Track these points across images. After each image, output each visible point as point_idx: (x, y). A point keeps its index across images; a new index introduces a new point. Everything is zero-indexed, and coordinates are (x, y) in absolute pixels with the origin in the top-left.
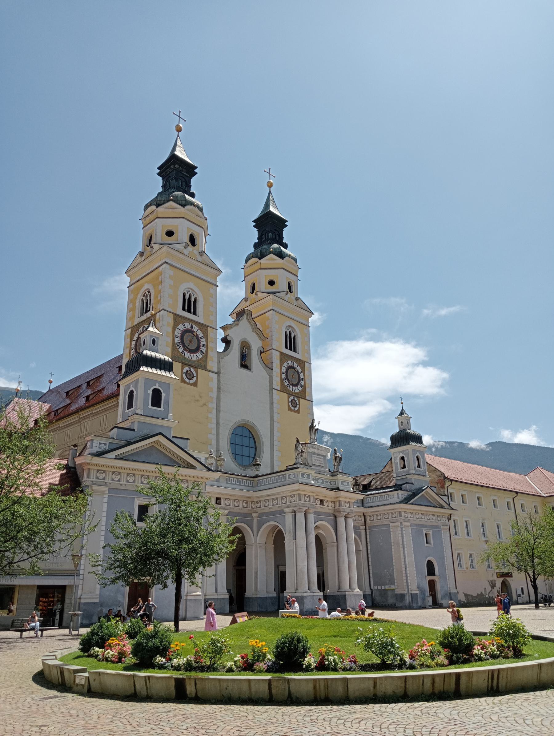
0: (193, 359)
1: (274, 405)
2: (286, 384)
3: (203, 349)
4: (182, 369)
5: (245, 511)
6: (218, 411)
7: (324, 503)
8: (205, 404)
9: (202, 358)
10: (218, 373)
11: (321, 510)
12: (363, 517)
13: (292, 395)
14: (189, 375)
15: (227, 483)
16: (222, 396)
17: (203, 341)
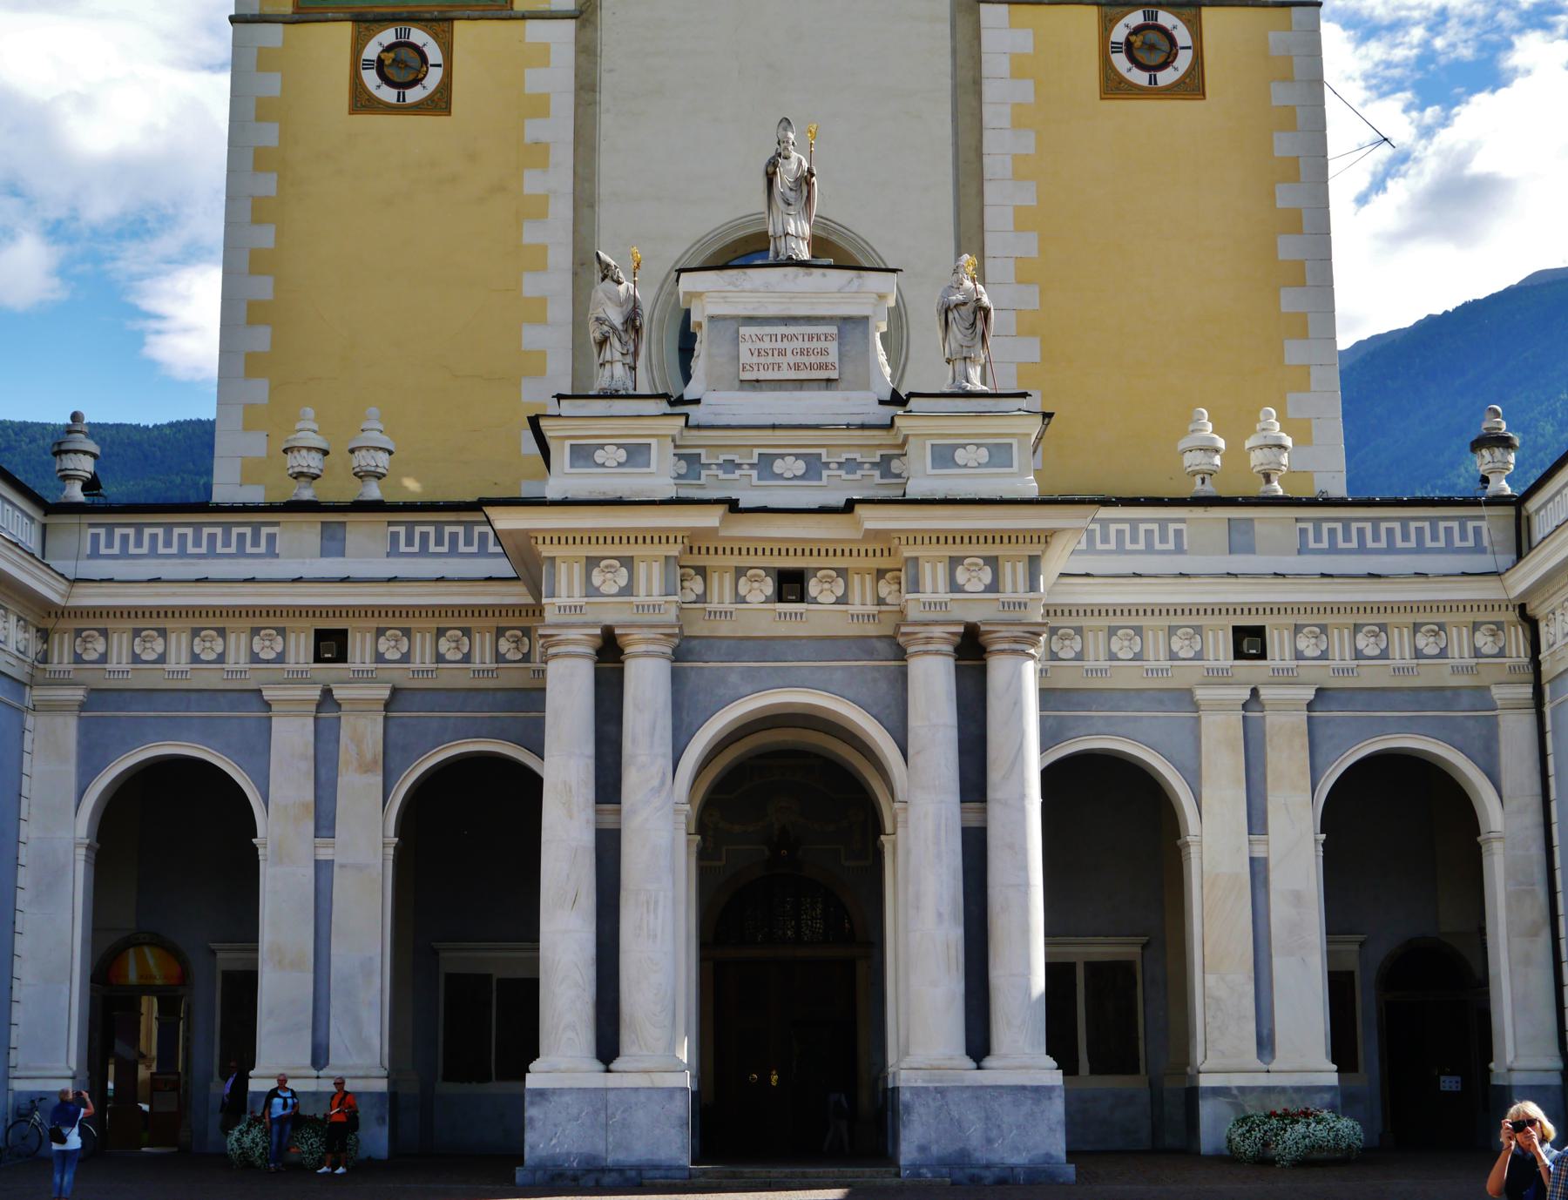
1: (990, 91)
4: (358, 46)
5: (512, 678)
6: (584, 201)
7: (813, 588)
11: (783, 629)
12: (1517, 641)
15: (393, 552)
16: (607, 123)
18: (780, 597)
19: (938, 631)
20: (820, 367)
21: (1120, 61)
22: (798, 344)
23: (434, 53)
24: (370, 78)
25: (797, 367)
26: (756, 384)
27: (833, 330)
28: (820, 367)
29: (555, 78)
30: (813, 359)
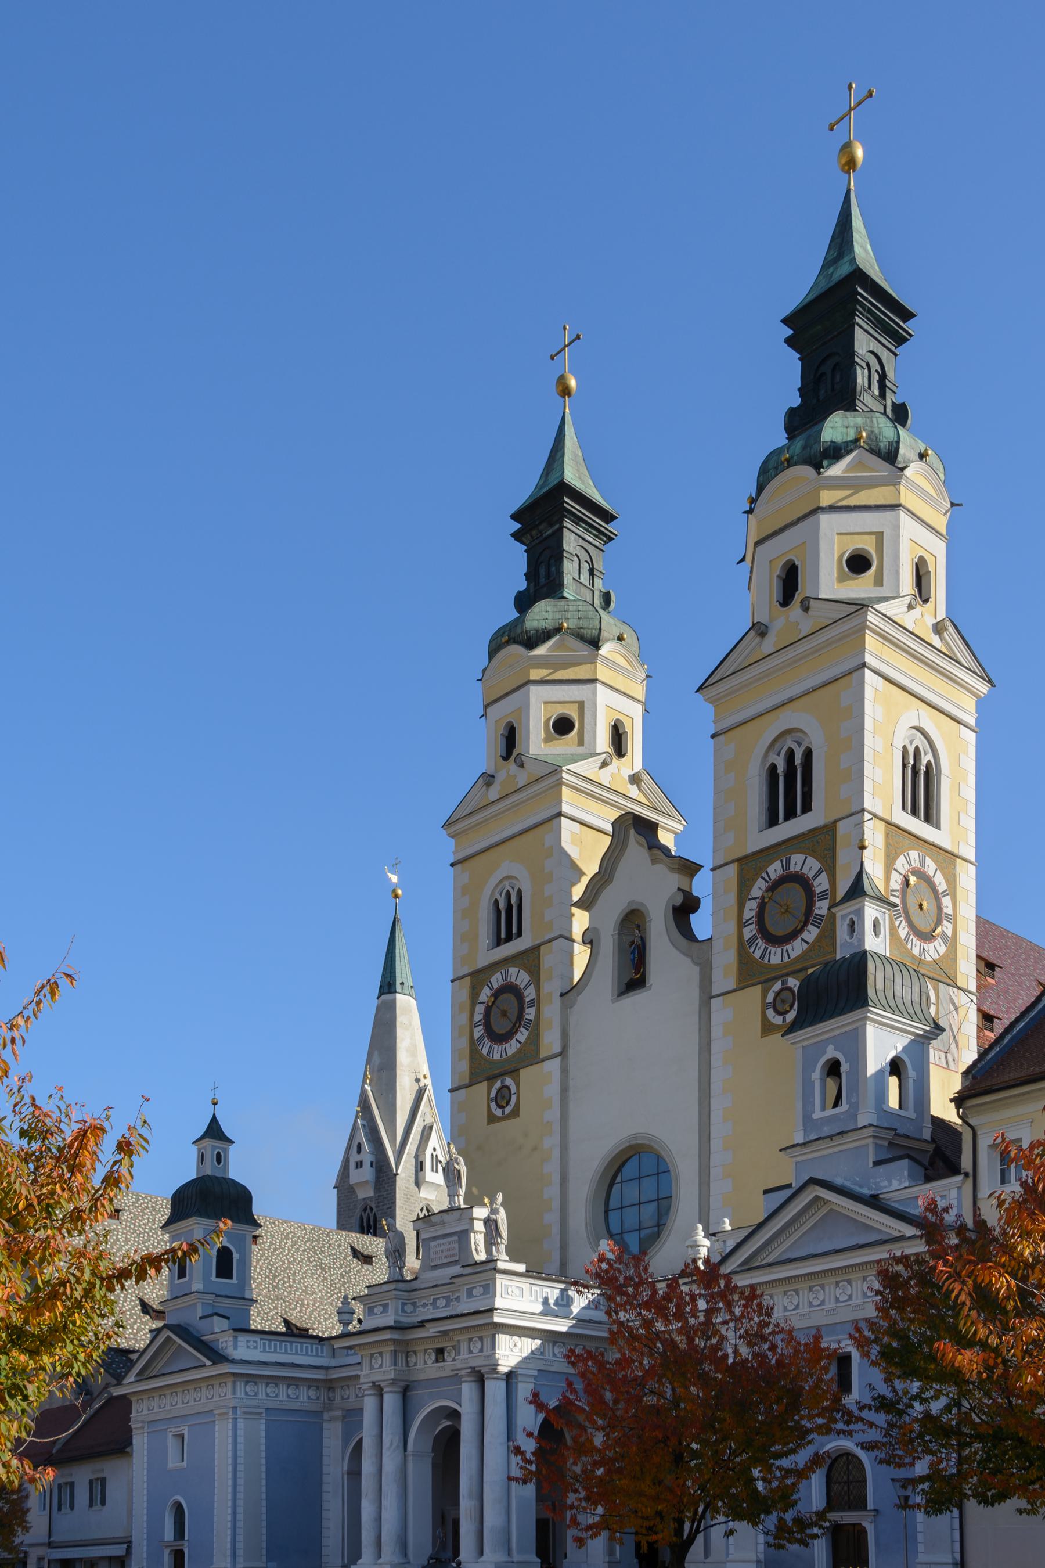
0: (510, 1052)
1: (715, 1047)
2: (757, 954)
3: (530, 1013)
8: (535, 1149)
9: (526, 1042)
10: (563, 1054)
13: (775, 979)
14: (503, 1097)
17: (530, 994)
18: (437, 1361)
19: (463, 1372)
20: (454, 1255)
21: (770, 1013)
22: (446, 1247)
23: (513, 1089)
24: (493, 1105)
25: (446, 1257)
26: (435, 1267)
27: (456, 1238)
28: (454, 1255)
29: (553, 1090)
30: (451, 1252)
